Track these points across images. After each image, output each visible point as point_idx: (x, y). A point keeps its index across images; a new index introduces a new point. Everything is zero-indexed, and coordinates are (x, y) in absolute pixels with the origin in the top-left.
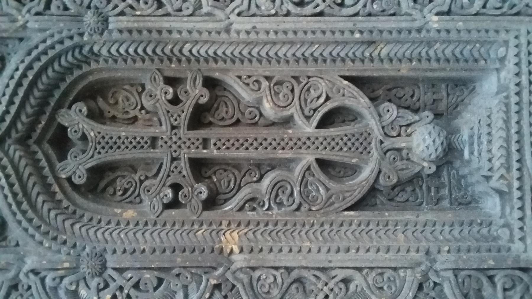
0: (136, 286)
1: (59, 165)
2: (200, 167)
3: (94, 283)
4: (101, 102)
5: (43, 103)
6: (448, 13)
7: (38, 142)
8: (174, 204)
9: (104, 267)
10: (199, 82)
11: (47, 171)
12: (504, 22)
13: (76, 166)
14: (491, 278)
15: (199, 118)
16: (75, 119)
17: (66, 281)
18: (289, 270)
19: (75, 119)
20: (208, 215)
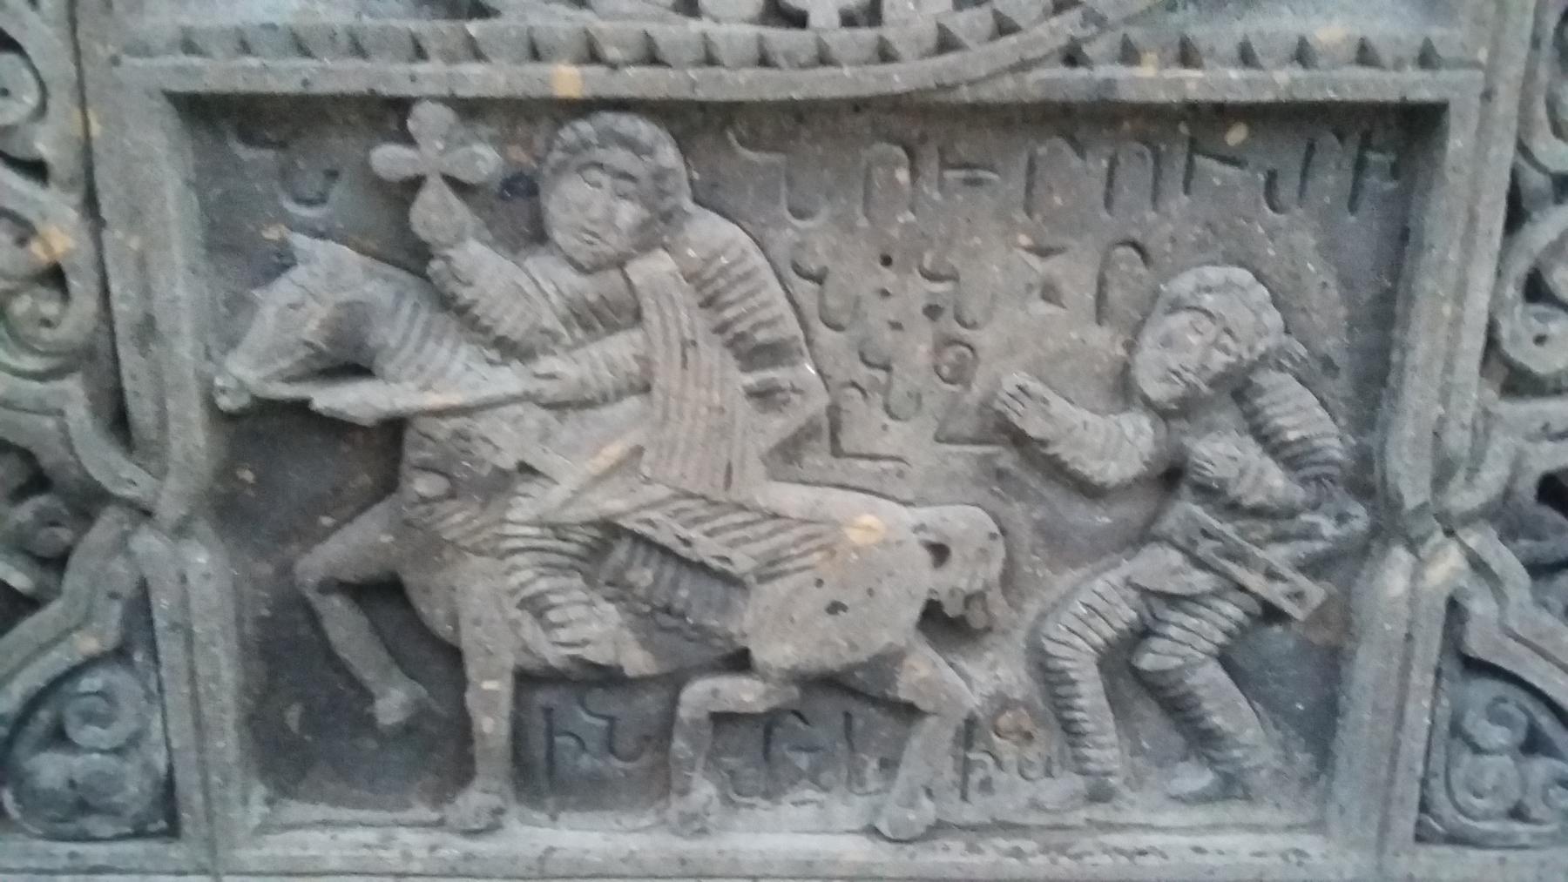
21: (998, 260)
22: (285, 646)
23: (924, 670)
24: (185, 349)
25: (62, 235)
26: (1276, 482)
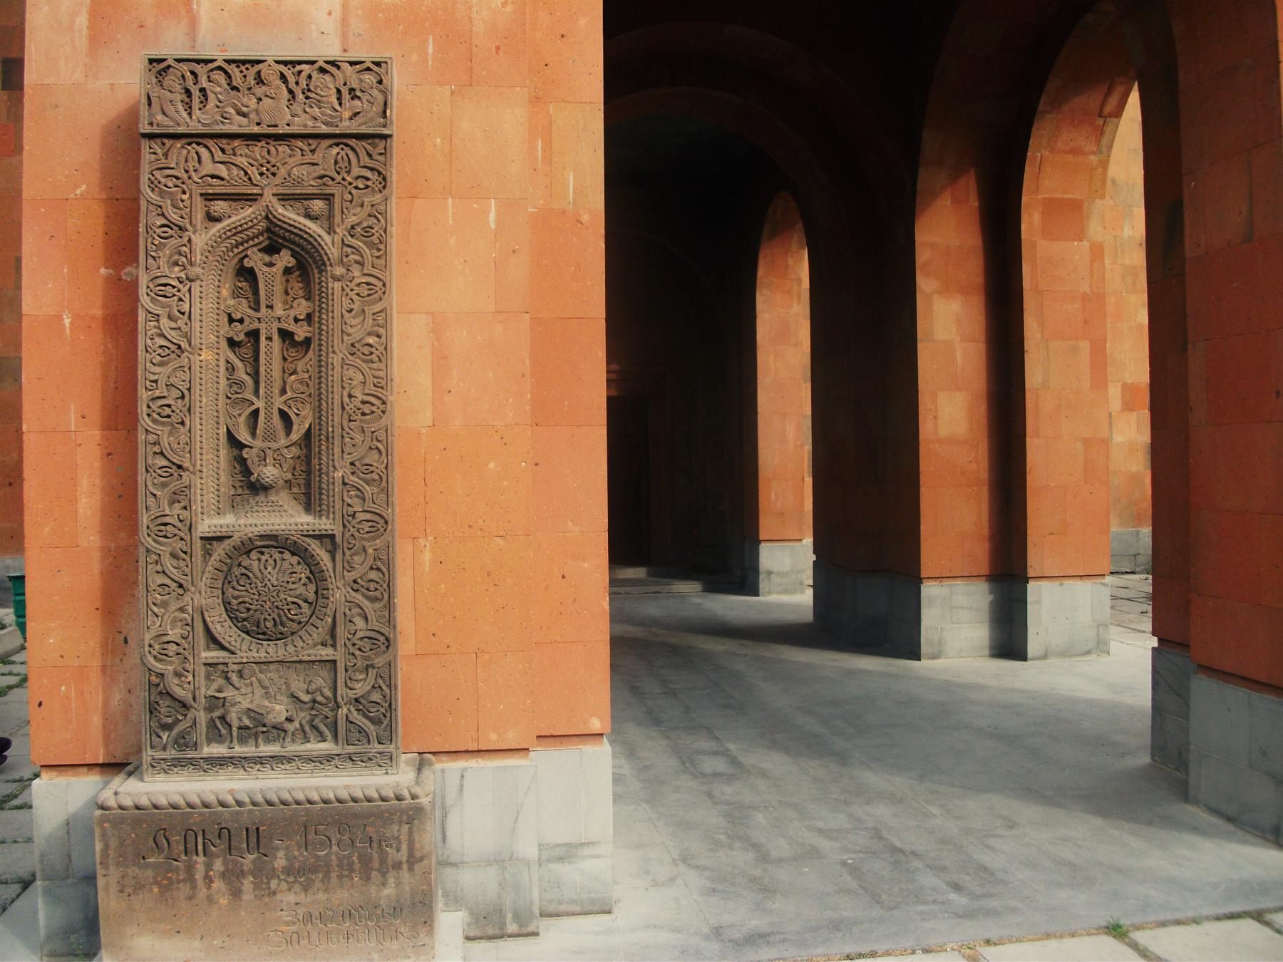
0: (180, 300)
1: (255, 249)
2: (254, 335)
3: (183, 275)
4: (297, 273)
5: (293, 243)
6: (345, 484)
7: (269, 238)
8: (231, 320)
9: (191, 281)
10: (308, 335)
11: (251, 243)
12: (339, 516)
13: (256, 260)
14: (185, 508)
15: (285, 335)
16: (285, 259)
17: (184, 259)
18: (189, 389)
19: (285, 259)
20: (224, 344)
21: (292, 676)
22: (212, 724)
23: (287, 726)
24: (203, 690)
25: (190, 678)
26: (324, 701)
